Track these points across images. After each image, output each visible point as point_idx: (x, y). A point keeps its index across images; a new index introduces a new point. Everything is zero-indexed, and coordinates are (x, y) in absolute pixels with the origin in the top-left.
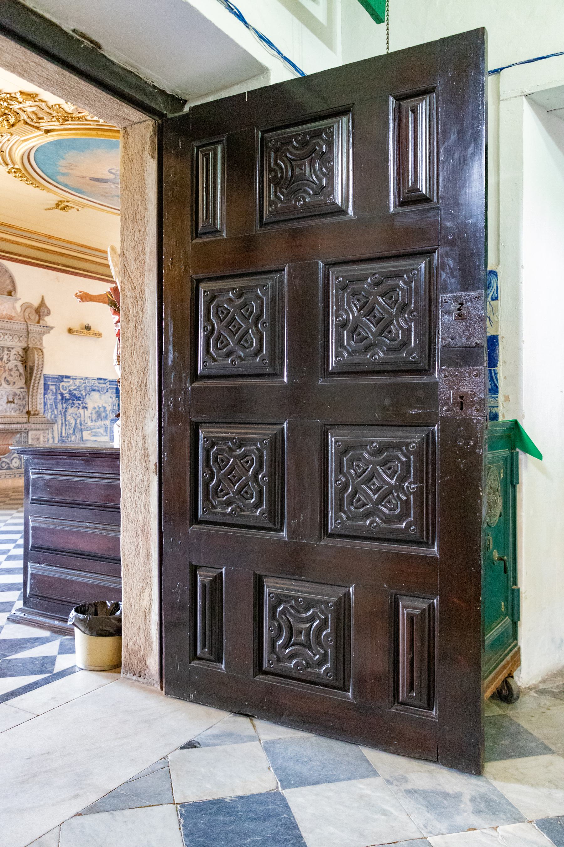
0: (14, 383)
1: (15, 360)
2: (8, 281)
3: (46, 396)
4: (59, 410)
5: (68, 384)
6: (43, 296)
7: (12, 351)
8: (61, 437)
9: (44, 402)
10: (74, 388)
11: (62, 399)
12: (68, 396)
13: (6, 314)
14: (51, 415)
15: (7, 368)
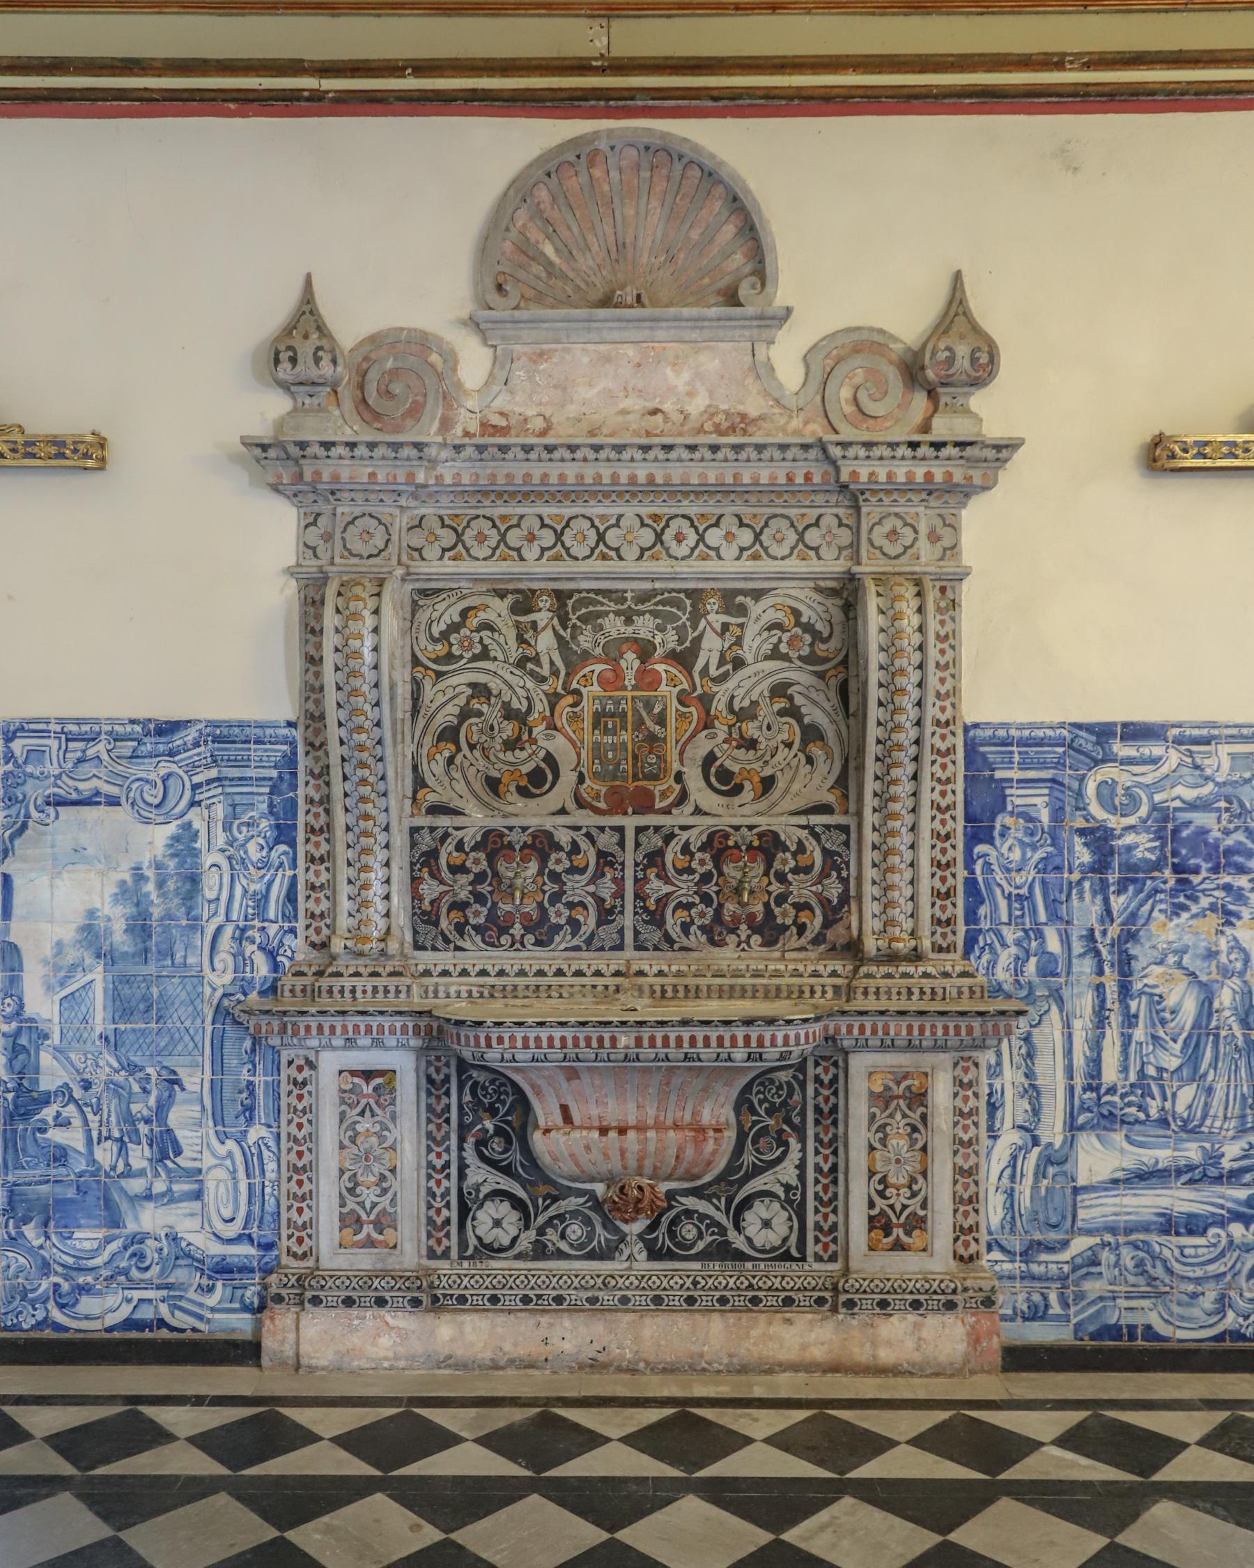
0: (768, 784)
1: (775, 654)
2: (729, 230)
3: (980, 848)
4: (1076, 933)
5: (1150, 775)
6: (958, 278)
7: (755, 608)
8: (1088, 1088)
9: (971, 883)
10: (1190, 795)
11: (1100, 867)
12: (1143, 846)
13: (710, 413)
14: (1020, 961)
15: (719, 705)
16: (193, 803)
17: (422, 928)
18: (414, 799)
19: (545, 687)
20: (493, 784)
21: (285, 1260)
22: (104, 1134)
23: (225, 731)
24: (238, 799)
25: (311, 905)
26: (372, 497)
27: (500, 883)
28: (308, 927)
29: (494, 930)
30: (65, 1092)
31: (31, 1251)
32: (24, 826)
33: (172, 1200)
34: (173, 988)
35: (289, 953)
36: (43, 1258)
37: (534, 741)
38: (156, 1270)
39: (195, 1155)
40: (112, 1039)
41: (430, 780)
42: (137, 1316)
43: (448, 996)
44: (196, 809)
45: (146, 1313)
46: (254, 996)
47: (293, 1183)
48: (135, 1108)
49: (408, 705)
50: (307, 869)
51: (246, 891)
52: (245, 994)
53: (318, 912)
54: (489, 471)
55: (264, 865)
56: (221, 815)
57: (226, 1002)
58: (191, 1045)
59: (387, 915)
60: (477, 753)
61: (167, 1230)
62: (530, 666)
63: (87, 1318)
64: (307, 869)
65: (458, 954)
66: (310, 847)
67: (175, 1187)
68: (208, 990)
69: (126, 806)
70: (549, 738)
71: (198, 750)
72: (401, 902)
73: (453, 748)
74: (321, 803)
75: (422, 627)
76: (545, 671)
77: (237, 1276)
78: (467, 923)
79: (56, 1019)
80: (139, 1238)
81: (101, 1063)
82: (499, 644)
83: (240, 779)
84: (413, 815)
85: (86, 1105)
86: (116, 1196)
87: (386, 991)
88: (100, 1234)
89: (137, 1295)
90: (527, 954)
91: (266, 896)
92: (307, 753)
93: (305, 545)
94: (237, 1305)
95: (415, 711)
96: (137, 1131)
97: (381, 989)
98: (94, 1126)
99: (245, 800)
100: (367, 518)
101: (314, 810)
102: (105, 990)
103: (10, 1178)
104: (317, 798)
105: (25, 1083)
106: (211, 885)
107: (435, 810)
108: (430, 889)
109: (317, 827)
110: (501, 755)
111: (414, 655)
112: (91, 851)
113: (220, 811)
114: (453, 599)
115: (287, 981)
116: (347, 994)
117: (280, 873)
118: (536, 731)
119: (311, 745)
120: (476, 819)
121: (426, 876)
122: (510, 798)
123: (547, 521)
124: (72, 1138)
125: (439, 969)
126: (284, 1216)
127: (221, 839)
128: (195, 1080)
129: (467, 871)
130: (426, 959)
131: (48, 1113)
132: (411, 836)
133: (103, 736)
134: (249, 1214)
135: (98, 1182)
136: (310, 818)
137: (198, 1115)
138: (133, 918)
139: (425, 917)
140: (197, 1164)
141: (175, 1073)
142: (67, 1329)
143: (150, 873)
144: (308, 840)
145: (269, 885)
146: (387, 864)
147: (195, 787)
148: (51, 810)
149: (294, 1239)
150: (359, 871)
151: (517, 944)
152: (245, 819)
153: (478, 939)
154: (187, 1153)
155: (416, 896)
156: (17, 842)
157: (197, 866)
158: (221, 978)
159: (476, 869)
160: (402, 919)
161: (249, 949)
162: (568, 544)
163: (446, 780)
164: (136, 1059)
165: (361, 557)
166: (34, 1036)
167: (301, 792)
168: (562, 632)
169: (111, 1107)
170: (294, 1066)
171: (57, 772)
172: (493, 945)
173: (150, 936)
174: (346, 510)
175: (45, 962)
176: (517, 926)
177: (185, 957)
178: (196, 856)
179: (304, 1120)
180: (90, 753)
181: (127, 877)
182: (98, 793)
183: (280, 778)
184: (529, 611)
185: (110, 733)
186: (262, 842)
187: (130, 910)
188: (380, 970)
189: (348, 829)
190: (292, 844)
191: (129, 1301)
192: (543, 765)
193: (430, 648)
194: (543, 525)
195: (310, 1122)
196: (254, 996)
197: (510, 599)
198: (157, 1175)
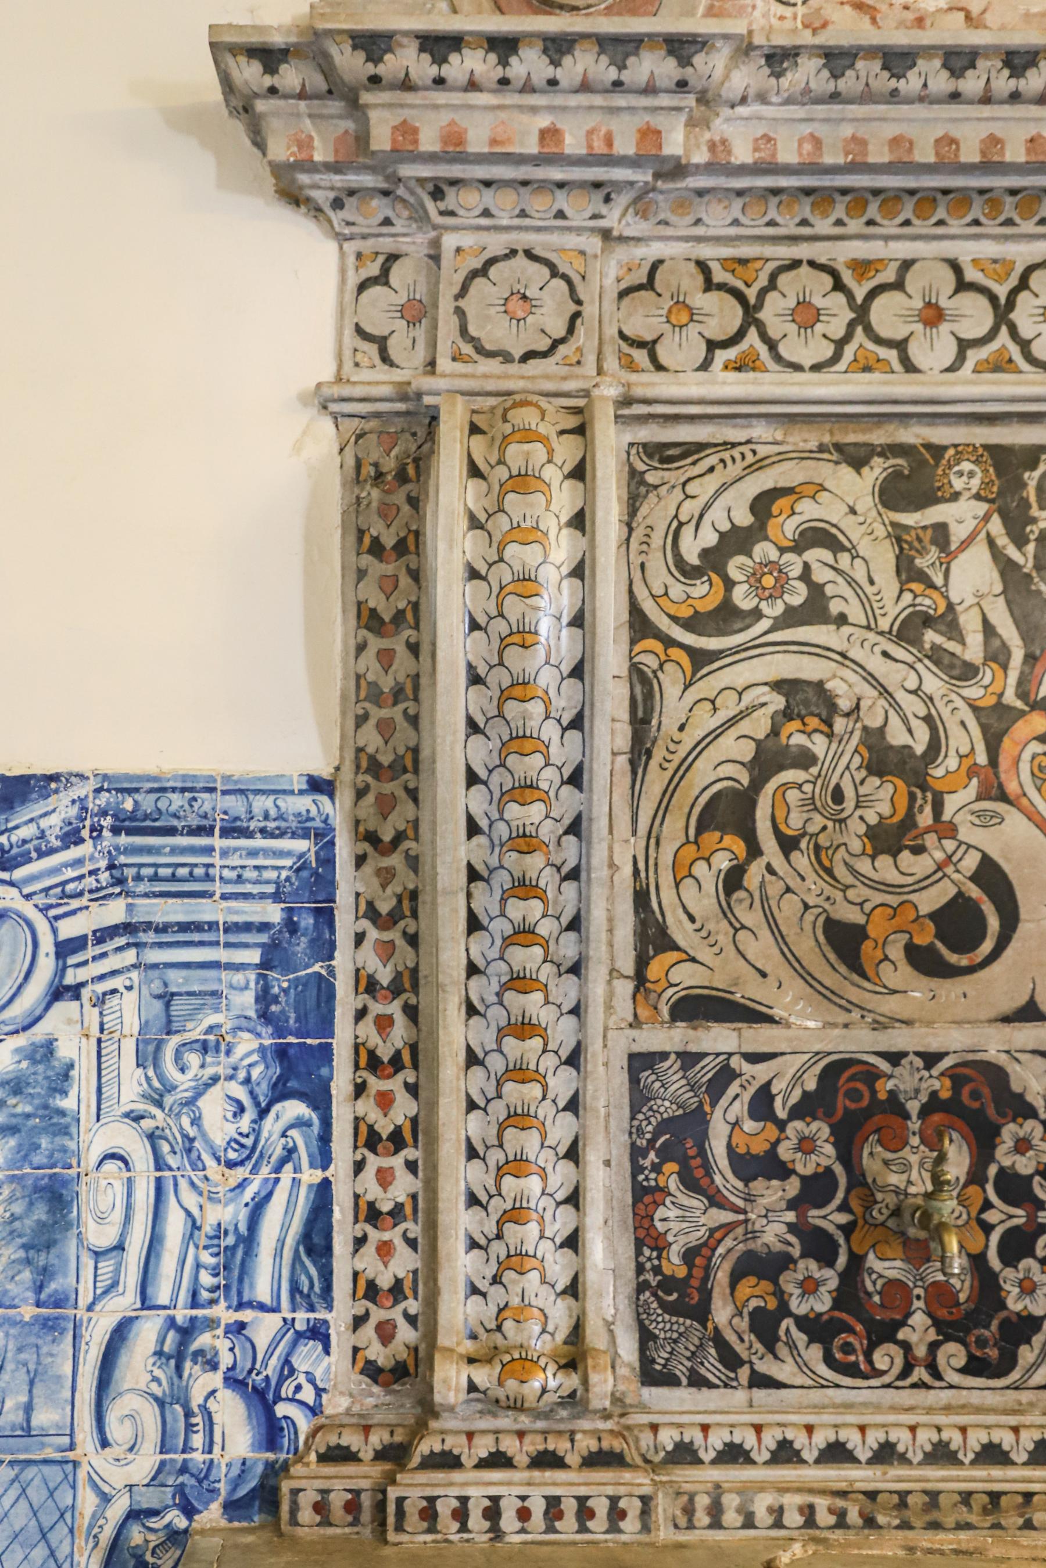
16: (59, 992)
17: (662, 1325)
18: (640, 978)
19: (973, 692)
20: (846, 942)
23: (148, 803)
24: (177, 979)
25: (368, 1262)
26: (540, 205)
27: (870, 1202)
28: (359, 1321)
29: (855, 1332)
35: (308, 1395)
37: (950, 831)
41: (680, 931)
43: (749, 1523)
44: (66, 1008)
46: (212, 1515)
49: (623, 738)
50: (359, 1167)
51: (195, 1227)
52: (189, 1511)
53: (385, 1282)
54: (847, 131)
55: (246, 1153)
56: (132, 1024)
57: (136, 1535)
59: (573, 1290)
60: (802, 860)
62: (931, 637)
64: (359, 1167)
65: (760, 1395)
66: (367, 1107)
68: (88, 1501)
70: (987, 821)
72: (607, 1256)
73: (739, 847)
74: (396, 990)
75: (657, 540)
76: (973, 650)
78: (784, 1310)
82: (851, 582)
83: (185, 927)
84: (636, 1023)
87: (585, 1513)
90: (945, 1396)
91: (249, 1240)
92: (360, 860)
93: (360, 332)
95: (639, 752)
97: (569, 1507)
100: (521, 260)
101: (377, 1008)
104: (385, 976)
106: (103, 1209)
107: (697, 1008)
108: (683, 1220)
109: (385, 1053)
110: (864, 866)
111: (635, 610)
113: (129, 1012)
114: (734, 470)
115: (308, 1479)
116: (476, 1521)
117: (287, 1175)
118: (951, 804)
119: (372, 838)
120: (805, 1033)
121: (673, 1183)
122: (889, 976)
123: (971, 275)
125: (717, 1440)
127: (130, 1085)
129: (782, 1171)
130: (677, 1408)
132: (634, 1080)
136: (367, 1030)
139: (672, 1294)
144: (360, 1089)
146: (573, 1154)
147: (65, 949)
150: (500, 1172)
151: (920, 1370)
152: (196, 1032)
153: (814, 1354)
155: (647, 1239)
157: (63, 1157)
158: (125, 1466)
159: (806, 1166)
160: (609, 1301)
161: (202, 1383)
162: (1026, 330)
163: (722, 930)
165: (507, 357)
167: (343, 961)
168: (1012, 552)
172: (851, 1370)
174: (467, 240)
176: (919, 1319)
177: (28, 1409)
178: (65, 1131)
183: (291, 926)
184: (929, 498)
186: (241, 1093)
188: (560, 1446)
189: (472, 1059)
190: (320, 1099)
192: (974, 892)
193: (677, 591)
194: (962, 286)
196: (212, 1515)
197: (877, 470)
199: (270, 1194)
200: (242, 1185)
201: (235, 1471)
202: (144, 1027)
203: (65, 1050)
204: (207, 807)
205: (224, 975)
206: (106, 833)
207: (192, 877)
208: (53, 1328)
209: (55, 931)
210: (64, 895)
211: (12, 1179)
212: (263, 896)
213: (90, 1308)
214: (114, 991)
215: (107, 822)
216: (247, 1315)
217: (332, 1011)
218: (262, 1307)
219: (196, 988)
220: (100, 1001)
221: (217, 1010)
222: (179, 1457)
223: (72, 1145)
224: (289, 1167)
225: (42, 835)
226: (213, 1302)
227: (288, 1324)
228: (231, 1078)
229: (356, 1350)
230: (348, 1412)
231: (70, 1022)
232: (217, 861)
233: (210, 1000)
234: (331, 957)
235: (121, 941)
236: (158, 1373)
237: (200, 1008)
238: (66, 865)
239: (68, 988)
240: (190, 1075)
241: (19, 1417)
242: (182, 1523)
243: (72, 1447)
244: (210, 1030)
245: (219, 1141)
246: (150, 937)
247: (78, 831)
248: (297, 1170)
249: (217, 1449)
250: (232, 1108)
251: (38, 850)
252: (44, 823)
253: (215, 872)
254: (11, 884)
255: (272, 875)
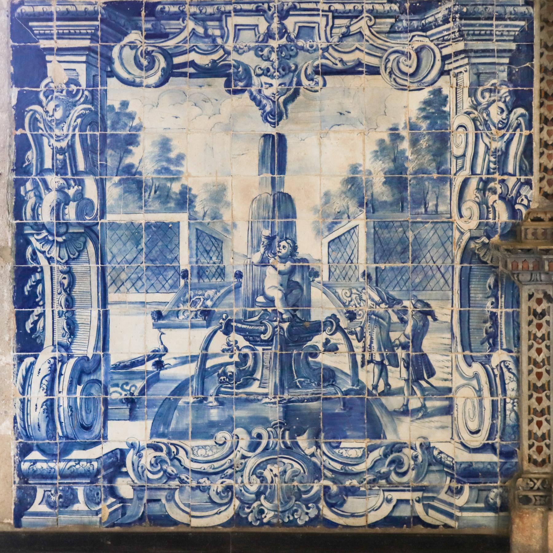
16: (443, 72)
21: (526, 466)
22: (367, 357)
23: (471, 9)
24: (482, 68)
30: (332, 322)
31: (304, 458)
32: (296, 93)
33: (426, 415)
34: (427, 232)
35: (525, 202)
36: (315, 464)
38: (412, 474)
39: (446, 376)
40: (374, 277)
42: (397, 514)
44: (445, 78)
45: (404, 512)
46: (496, 239)
47: (533, 400)
48: (394, 336)
50: (541, 130)
51: (488, 148)
52: (489, 238)
55: (505, 125)
56: (467, 83)
57: (472, 245)
58: (442, 281)
61: (422, 440)
63: (353, 515)
67: (429, 404)
68: (457, 234)
69: (385, 74)
71: (447, 26)
77: (482, 480)
79: (325, 259)
80: (396, 447)
81: (364, 297)
83: (484, 51)
85: (352, 333)
86: (377, 412)
88: (364, 444)
89: (396, 496)
91: (506, 153)
92: (542, 28)
94: (482, 505)
96: (396, 355)
98: (358, 351)
99: (488, 69)
102: (368, 234)
103: (286, 396)
105: (298, 314)
106: (458, 144)
112: (354, 114)
113: (466, 79)
117: (518, 132)
124: (339, 361)
126: (525, 428)
127: (467, 103)
128: (446, 311)
131: (318, 340)
133: (365, 14)
134: (493, 427)
135: (362, 399)
137: (448, 342)
138: (390, 172)
140: (447, 384)
141: (428, 305)
142: (336, 525)
143: (405, 133)
145: (509, 143)
147: (445, 58)
148: (319, 78)
149: (534, 449)
152: (488, 86)
154: (439, 374)
156: (290, 107)
157: (445, 126)
158: (468, 223)
161: (492, 198)
164: (395, 293)
166: (306, 274)
167: (536, 62)
169: (373, 334)
170: (534, 299)
171: (324, 45)
173: (406, 188)
175: (316, 211)
177: (437, 206)
179: (543, 346)
180: (353, 29)
181: (386, 137)
182: (360, 64)
185: (370, 11)
186: (503, 106)
187: (389, 165)
190: (529, 108)
191: (389, 501)
195: (548, 347)
196: (496, 239)
198: (413, 393)
199: (512, 139)
200: (504, 135)
201: (503, 226)
202: (471, 84)
203: (445, 92)
204: (491, 10)
205: (497, 67)
206: (457, 20)
207: (486, 34)
208: (443, 181)
209: (441, 52)
210: (444, 40)
211: (428, 133)
212: (509, 41)
213: (455, 174)
214: (461, 72)
215: (458, 16)
216: (505, 177)
217: (532, 78)
218: (510, 175)
219: (488, 71)
220: (456, 75)
221: (495, 78)
222: (485, 221)
223: (448, 123)
224: (518, 130)
225: (436, 20)
226: (494, 173)
227: (519, 180)
228: (499, 101)
229: (540, 188)
230: (538, 207)
231: (446, 82)
232: (494, 28)
233: (492, 75)
234: (532, 61)
235: (463, 56)
236: (478, 195)
237: (489, 78)
238: (444, 30)
239: (446, 71)
240: (486, 100)
241: (434, 208)
242: (487, 241)
243: (451, 217)
244: (493, 85)
245: (496, 121)
246: (472, 54)
247: (448, 19)
248: (521, 130)
249: (497, 219)
250: (500, 111)
251: (435, 25)
252: (437, 16)
253: (494, 32)
254: (426, 37)
255: (513, 33)
